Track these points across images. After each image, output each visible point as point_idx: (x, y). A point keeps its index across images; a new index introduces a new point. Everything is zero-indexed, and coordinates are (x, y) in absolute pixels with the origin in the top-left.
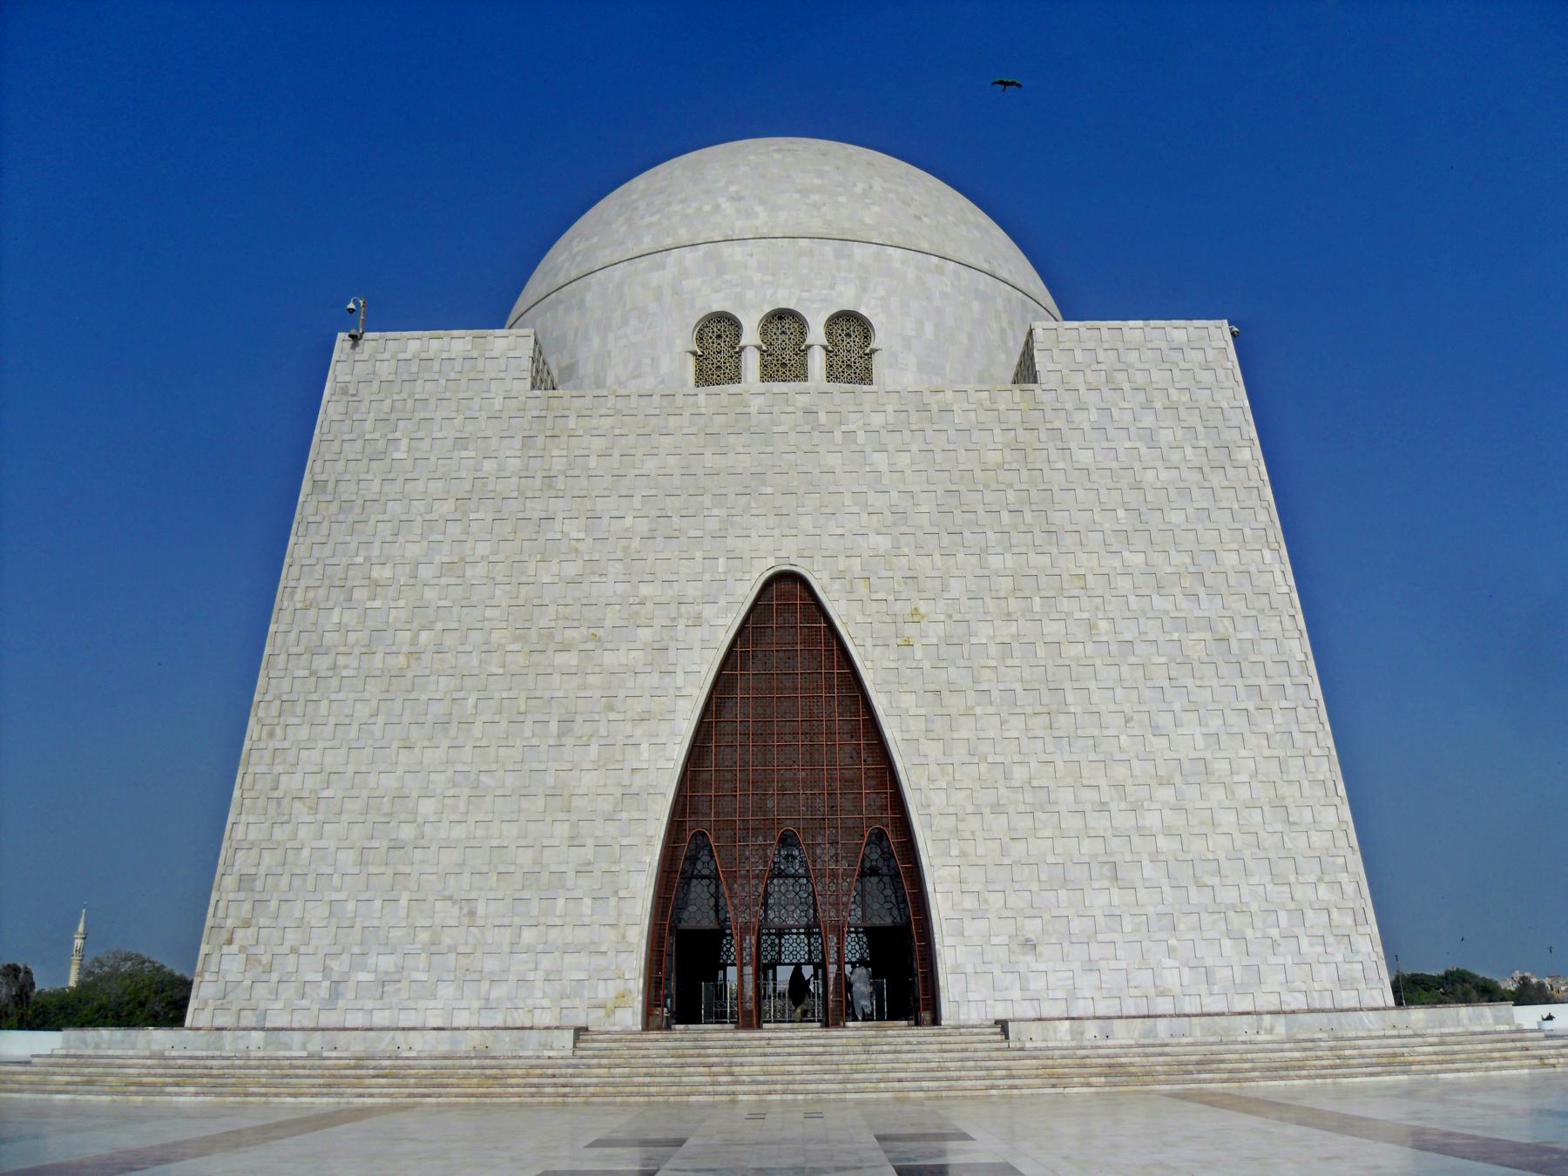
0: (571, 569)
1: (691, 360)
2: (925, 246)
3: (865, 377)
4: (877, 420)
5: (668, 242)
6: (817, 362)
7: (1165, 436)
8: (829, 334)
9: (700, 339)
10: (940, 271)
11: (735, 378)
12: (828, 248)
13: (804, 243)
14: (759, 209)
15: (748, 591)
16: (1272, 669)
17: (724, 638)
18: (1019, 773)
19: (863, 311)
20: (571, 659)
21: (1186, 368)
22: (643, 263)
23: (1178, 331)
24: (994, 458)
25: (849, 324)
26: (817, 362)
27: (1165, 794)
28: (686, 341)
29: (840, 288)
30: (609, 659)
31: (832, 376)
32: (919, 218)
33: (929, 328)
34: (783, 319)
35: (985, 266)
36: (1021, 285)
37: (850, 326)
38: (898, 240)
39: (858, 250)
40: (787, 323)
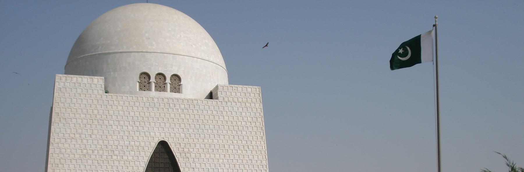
1: (138, 83)
2: (193, 55)
5: (131, 50)
7: (244, 114)
8: (171, 79)
9: (140, 78)
11: (149, 89)
13: (165, 55)
14: (154, 43)
15: (154, 145)
16: (260, 167)
19: (179, 74)
21: (250, 96)
22: (125, 54)
23: (249, 89)
26: (169, 86)
28: (137, 78)
29: (174, 68)
32: (192, 46)
34: (161, 76)
36: (215, 62)
37: (176, 78)
38: (187, 54)
40: (161, 76)
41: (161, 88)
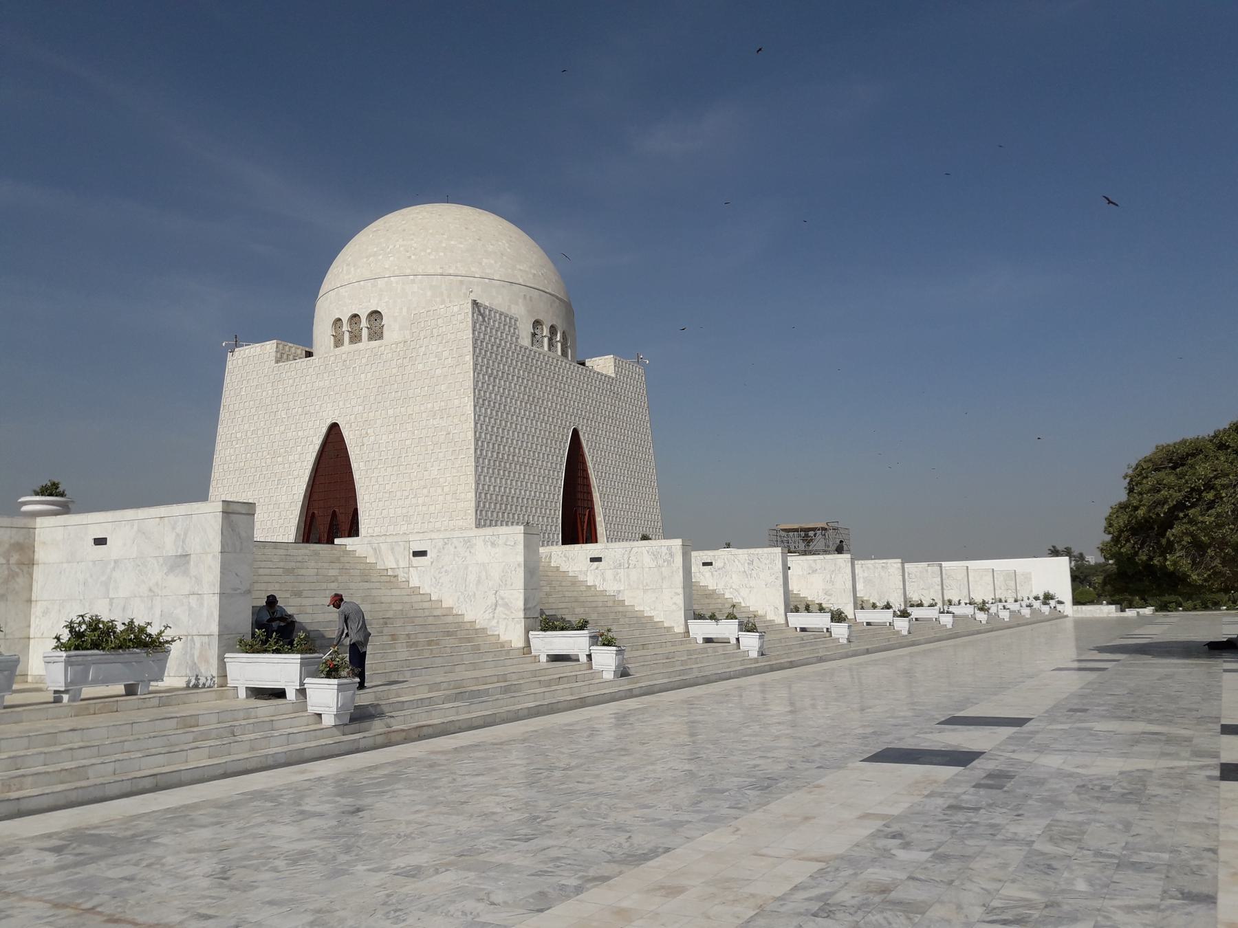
0: (282, 428)
2: (408, 271)
3: (381, 337)
4: (364, 361)
6: (365, 333)
10: (413, 281)
12: (369, 284)
15: (324, 430)
17: (317, 447)
18: (388, 487)
20: (280, 459)
24: (394, 371)
25: (375, 315)
26: (365, 333)
27: (425, 491)
30: (291, 458)
31: (370, 339)
33: (405, 310)
34: (356, 316)
35: (440, 271)
37: (375, 315)
38: (397, 273)
39: (379, 281)
41: (355, 338)
